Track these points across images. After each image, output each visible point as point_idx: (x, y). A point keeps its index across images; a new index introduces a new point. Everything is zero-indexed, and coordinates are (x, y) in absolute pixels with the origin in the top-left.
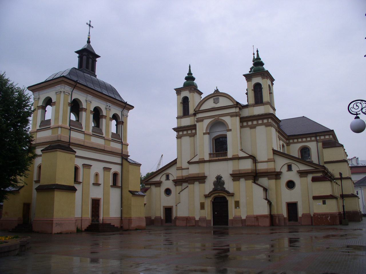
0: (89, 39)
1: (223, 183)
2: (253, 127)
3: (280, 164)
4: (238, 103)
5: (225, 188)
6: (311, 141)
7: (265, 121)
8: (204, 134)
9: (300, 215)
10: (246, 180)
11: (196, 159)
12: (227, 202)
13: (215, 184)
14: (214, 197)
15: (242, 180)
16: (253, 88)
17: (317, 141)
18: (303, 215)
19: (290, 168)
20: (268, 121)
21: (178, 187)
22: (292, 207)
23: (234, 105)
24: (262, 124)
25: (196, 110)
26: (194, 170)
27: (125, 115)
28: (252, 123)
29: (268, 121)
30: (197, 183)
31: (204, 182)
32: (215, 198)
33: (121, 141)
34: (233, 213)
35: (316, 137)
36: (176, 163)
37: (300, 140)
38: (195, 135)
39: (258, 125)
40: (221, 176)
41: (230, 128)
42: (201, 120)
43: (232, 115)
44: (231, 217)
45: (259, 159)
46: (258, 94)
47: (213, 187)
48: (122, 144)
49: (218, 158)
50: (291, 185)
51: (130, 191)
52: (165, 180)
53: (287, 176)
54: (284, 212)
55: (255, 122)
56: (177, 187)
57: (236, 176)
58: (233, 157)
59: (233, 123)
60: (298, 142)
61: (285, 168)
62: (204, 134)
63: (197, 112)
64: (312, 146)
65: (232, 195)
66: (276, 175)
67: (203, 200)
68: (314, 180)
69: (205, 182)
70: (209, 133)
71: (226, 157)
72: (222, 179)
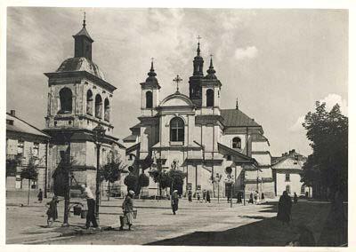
45: (206, 149)
64: (243, 137)
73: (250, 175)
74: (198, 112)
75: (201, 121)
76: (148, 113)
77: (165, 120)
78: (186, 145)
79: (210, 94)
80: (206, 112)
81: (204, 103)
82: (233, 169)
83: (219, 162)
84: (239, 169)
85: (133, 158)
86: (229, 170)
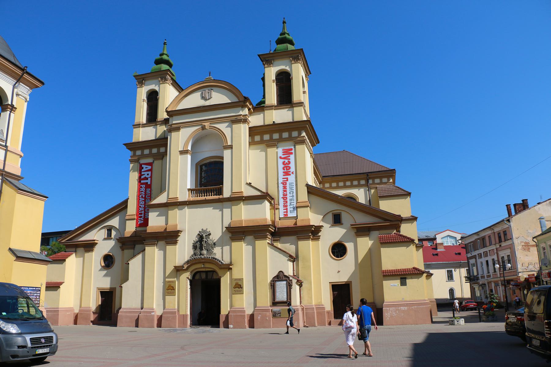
2: (272, 144)
4: (246, 99)
5: (215, 254)
6: (359, 186)
7: (295, 134)
13: (195, 247)
14: (194, 270)
16: (274, 78)
20: (300, 134)
21: (126, 251)
23: (240, 102)
24: (290, 139)
25: (169, 110)
27: (20, 93)
31: (175, 243)
33: (4, 144)
36: (126, 207)
39: (281, 140)
40: (208, 230)
41: (229, 143)
44: (225, 309)
47: (192, 252)
48: (6, 151)
49: (206, 197)
51: (10, 249)
52: (105, 239)
54: (326, 301)
55: (276, 136)
56: (125, 251)
58: (233, 196)
63: (171, 113)
65: (228, 267)
66: (313, 232)
69: (177, 243)
71: (221, 197)
72: (211, 237)
73: (394, 258)
74: (256, 120)
75: (263, 136)
76: (146, 134)
77: (180, 140)
78: (227, 193)
79: (284, 81)
80: (282, 116)
81: (272, 97)
82: (350, 246)
83: (313, 232)
84: (365, 243)
85: (114, 233)
86: (338, 250)
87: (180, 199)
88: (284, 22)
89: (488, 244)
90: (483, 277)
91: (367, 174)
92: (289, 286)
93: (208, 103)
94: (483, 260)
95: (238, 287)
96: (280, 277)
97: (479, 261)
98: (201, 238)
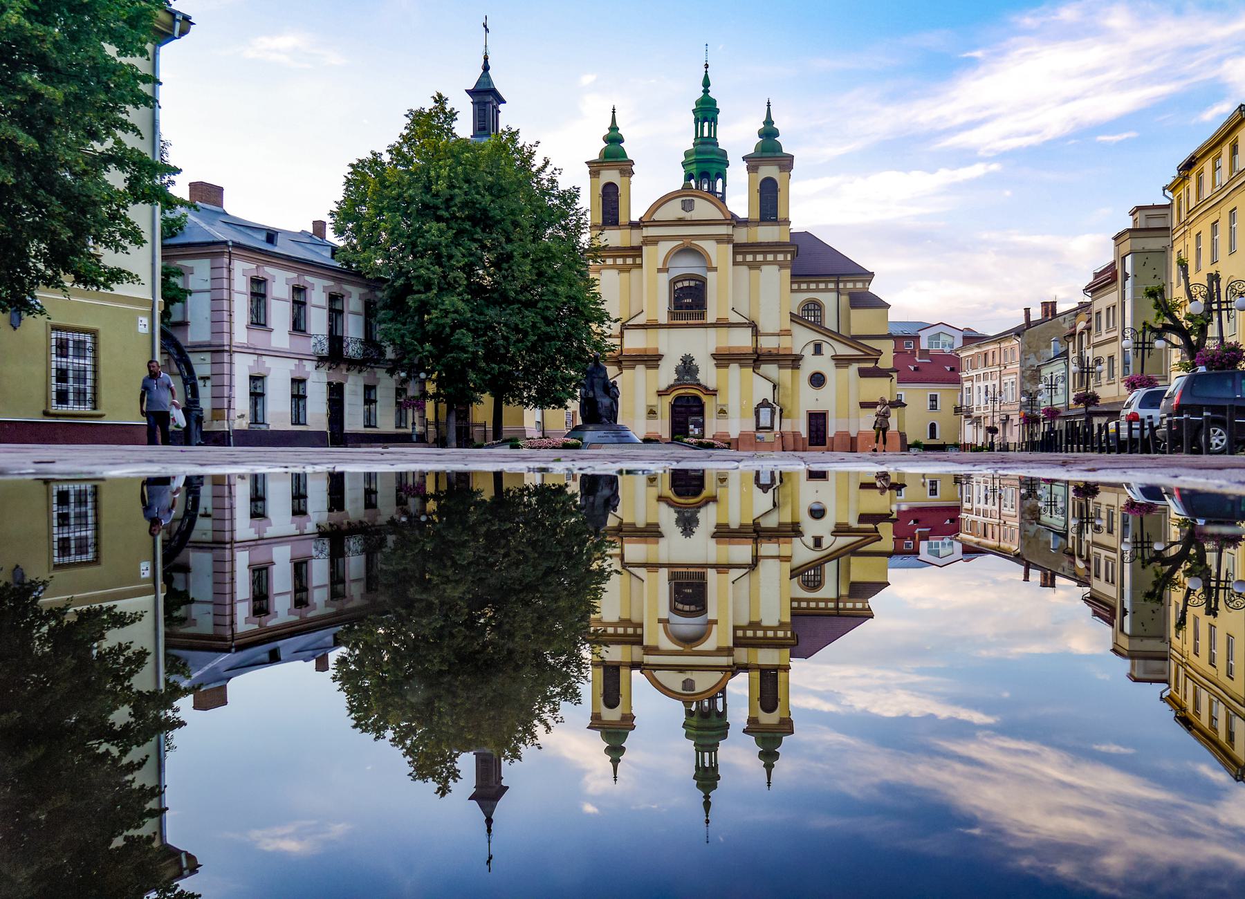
0: (486, 59)
1: (697, 371)
2: (754, 266)
3: (801, 340)
6: (826, 290)
7: (780, 257)
8: (660, 270)
9: (831, 433)
10: (742, 366)
11: (640, 320)
12: (701, 406)
15: (734, 367)
17: (838, 291)
18: (837, 434)
19: (818, 350)
20: (785, 257)
22: (818, 421)
26: (634, 342)
28: (755, 258)
29: (785, 257)
30: (640, 368)
31: (657, 367)
32: (678, 398)
34: (713, 427)
35: (837, 283)
37: (804, 286)
38: (635, 272)
39: (765, 262)
42: (654, 241)
43: (719, 239)
46: (769, 200)
50: (817, 380)
53: (812, 364)
55: (760, 258)
57: (723, 359)
59: (719, 254)
60: (799, 290)
61: (811, 348)
62: (660, 270)
64: (828, 300)
65: (714, 393)
66: (794, 361)
67: (654, 400)
68: (864, 373)
70: (667, 270)
87: (660, 322)
88: (769, 105)
89: (990, 363)
90: (978, 408)
91: (838, 275)
92: (773, 413)
93: (688, 216)
94: (982, 384)
95: (723, 412)
96: (765, 404)
97: (976, 385)
98: (684, 362)
